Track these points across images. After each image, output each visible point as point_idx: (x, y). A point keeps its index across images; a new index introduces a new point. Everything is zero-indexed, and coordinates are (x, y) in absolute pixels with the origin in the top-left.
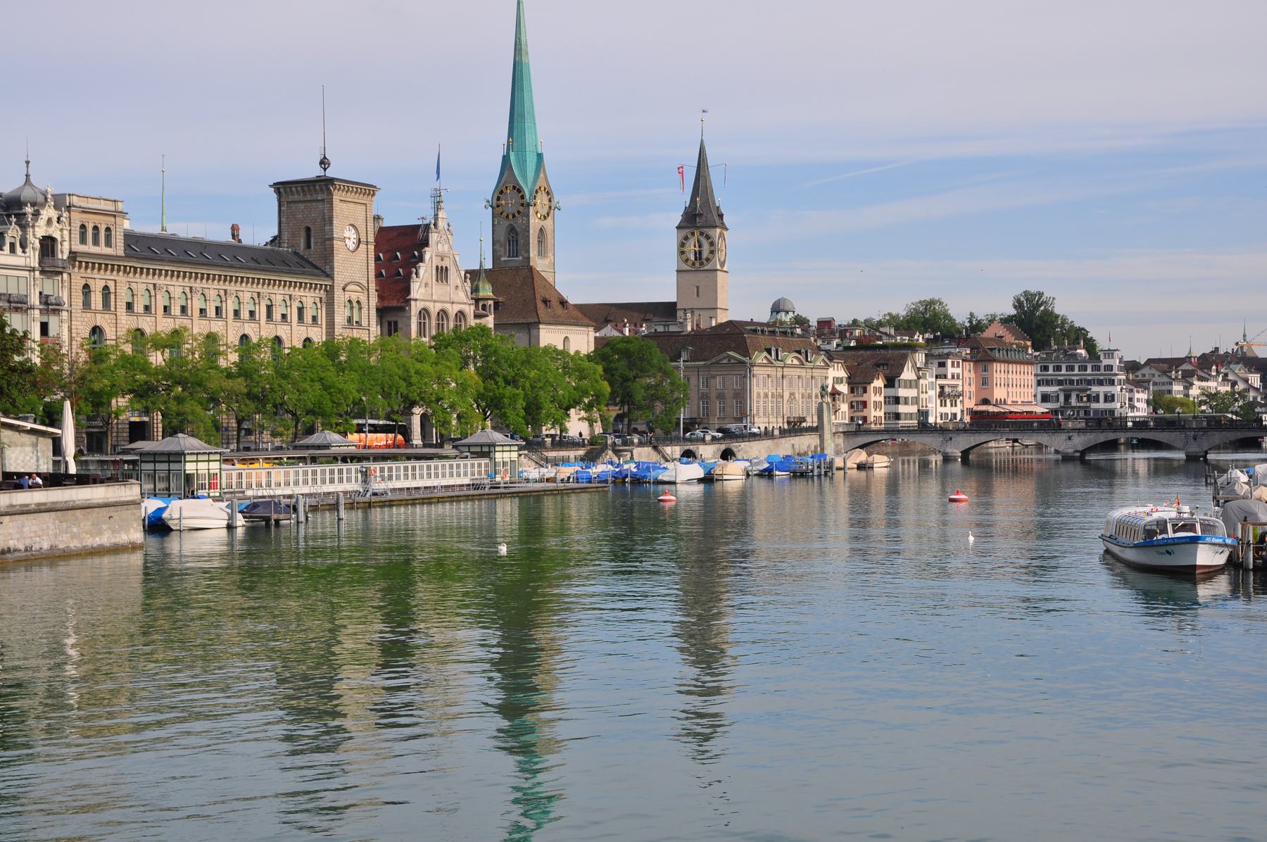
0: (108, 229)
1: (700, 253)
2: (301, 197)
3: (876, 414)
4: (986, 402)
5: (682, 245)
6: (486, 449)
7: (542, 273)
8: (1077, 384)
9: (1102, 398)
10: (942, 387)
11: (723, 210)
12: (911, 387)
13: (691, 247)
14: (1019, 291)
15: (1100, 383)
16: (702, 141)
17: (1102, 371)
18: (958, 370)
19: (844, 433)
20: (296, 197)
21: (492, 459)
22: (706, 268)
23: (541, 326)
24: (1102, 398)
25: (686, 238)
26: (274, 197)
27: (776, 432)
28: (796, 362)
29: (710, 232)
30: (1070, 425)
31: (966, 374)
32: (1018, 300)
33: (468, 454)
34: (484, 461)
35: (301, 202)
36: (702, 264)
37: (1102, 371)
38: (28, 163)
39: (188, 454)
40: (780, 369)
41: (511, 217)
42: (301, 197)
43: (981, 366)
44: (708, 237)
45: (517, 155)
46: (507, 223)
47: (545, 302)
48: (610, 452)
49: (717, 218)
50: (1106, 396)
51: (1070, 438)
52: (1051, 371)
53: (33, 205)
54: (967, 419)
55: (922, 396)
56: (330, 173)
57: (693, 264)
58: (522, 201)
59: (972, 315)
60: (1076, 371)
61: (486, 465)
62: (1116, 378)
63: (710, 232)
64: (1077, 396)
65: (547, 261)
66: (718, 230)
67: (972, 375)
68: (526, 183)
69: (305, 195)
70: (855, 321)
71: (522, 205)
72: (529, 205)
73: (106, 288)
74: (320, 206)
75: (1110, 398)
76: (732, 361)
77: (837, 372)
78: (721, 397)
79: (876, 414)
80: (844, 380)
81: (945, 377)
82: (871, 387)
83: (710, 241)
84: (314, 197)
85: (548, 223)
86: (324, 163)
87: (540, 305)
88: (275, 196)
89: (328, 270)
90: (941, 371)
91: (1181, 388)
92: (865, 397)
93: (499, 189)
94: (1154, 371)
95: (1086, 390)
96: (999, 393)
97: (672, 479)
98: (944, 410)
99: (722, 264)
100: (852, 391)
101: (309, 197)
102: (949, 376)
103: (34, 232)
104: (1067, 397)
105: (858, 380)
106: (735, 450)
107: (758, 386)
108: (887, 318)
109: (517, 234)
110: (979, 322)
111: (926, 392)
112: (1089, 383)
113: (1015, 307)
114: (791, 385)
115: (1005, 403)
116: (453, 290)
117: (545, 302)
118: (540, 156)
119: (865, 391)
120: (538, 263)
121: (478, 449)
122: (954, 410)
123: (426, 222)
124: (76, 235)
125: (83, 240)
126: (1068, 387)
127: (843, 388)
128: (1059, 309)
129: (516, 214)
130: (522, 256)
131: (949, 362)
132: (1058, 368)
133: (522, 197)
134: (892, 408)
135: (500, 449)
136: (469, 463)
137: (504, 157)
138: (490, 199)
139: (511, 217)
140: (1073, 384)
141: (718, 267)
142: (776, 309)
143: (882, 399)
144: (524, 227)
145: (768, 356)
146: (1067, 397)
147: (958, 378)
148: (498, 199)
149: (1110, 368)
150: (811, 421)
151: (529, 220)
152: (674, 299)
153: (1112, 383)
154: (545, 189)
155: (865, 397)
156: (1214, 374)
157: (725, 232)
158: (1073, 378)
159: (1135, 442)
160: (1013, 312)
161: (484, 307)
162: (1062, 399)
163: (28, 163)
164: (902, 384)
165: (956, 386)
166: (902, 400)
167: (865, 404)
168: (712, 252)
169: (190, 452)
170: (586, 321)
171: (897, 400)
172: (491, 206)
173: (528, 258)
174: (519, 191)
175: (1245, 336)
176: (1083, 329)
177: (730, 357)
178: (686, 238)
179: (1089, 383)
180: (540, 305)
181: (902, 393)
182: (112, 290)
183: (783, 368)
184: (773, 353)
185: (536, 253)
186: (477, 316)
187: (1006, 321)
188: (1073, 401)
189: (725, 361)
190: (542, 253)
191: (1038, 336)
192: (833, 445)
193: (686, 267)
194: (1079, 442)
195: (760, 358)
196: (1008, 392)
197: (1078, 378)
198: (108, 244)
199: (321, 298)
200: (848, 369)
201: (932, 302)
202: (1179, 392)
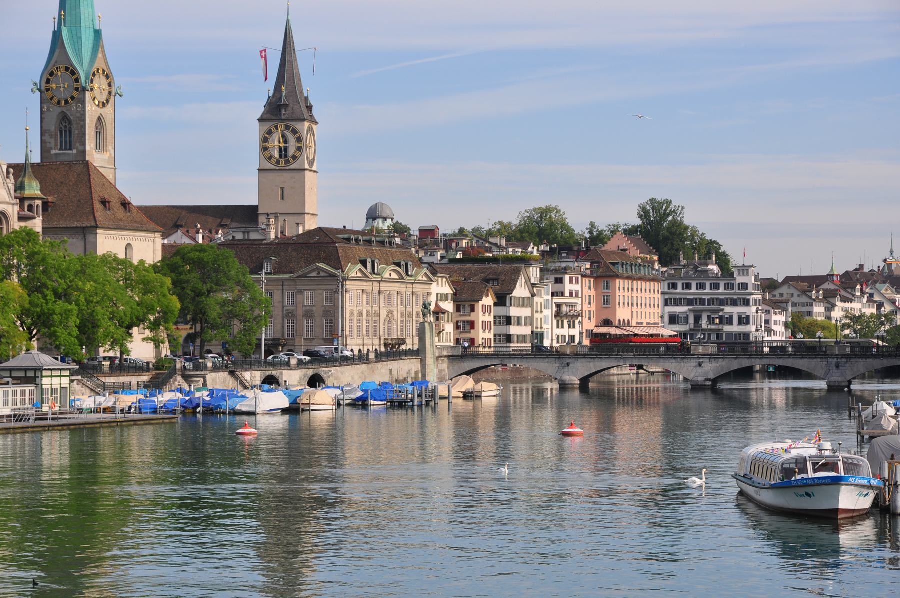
1: (286, 149)
3: (484, 336)
4: (607, 323)
5: (265, 140)
6: (31, 374)
7: (100, 170)
8: (709, 304)
9: (735, 320)
10: (559, 306)
11: (312, 101)
12: (524, 306)
13: (276, 142)
14: (644, 199)
15: (734, 303)
16: (288, 21)
17: (736, 290)
18: (577, 287)
19: (449, 357)
21: (39, 386)
22: (292, 167)
23: (99, 231)
24: (735, 320)
25: (270, 132)
27: (372, 356)
28: (395, 276)
29: (298, 126)
30: (701, 350)
31: (586, 292)
32: (644, 209)
33: (10, 380)
34: (28, 388)
36: (287, 162)
37: (736, 290)
39: (46, 369)
40: (376, 284)
41: (63, 103)
43: (602, 283)
44: (295, 132)
45: (70, 31)
46: (59, 110)
47: (104, 203)
48: (179, 378)
49: (305, 110)
50: (740, 318)
51: (700, 365)
52: (679, 290)
54: (587, 342)
55: (536, 316)
57: (278, 162)
58: (76, 85)
59: (592, 225)
60: (708, 290)
61: (31, 393)
62: (751, 298)
63: (298, 126)
64: (709, 317)
65: (106, 156)
66: (307, 124)
67: (593, 293)
68: (81, 63)
70: (462, 231)
71: (77, 89)
72: (84, 90)
75: (744, 320)
76: (322, 274)
77: (442, 287)
78: (309, 315)
79: (484, 336)
80: (450, 297)
81: (563, 294)
82: (479, 306)
83: (297, 136)
85: (108, 112)
87: (98, 206)
90: (558, 287)
91: (822, 310)
92: (472, 317)
93: (49, 71)
94: (793, 291)
95: (718, 311)
96: (622, 314)
97: (252, 409)
98: (560, 332)
99: (311, 163)
100: (458, 309)
102: (567, 294)
104: (698, 319)
105: (465, 297)
106: (324, 376)
107: (351, 302)
108: (498, 227)
109: (70, 123)
110: (601, 233)
111: (541, 312)
112: (722, 303)
113: (640, 217)
114: (389, 302)
115: (629, 324)
117: (104, 203)
118: (98, 34)
119: (473, 310)
120: (96, 158)
121: (22, 374)
122: (573, 332)
126: (699, 307)
127: (449, 306)
128: (689, 220)
129: (70, 100)
130: (77, 149)
131: (567, 278)
132: (688, 286)
133: (77, 80)
134: (503, 330)
135: (49, 374)
136: (10, 390)
137: (55, 33)
138: (38, 82)
139: (63, 103)
140: (704, 304)
141: (307, 167)
142: (373, 215)
143: (492, 319)
144: (78, 115)
145: (364, 269)
146: (698, 319)
147: (577, 296)
148: (48, 81)
149: (744, 286)
150: (412, 344)
151: (84, 108)
152: (253, 201)
153: (747, 303)
154: (104, 71)
155: (472, 317)
156: (858, 294)
157: (314, 127)
158: (704, 297)
159: (772, 369)
160: (638, 222)
161: (30, 208)
162: (691, 320)
164: (514, 302)
165: (573, 306)
166: (514, 321)
167: (472, 325)
168: (299, 149)
169: (47, 368)
170: (153, 226)
171: (508, 321)
172: (40, 90)
173: (84, 152)
174: (73, 73)
175: (892, 252)
176: (715, 242)
177: (319, 270)
178: (270, 132)
179: (722, 303)
180: (98, 206)
181: (514, 312)
183: (379, 282)
184: (369, 265)
185: (93, 145)
186: (21, 219)
187: (630, 232)
188: (704, 324)
189: (314, 274)
190: (100, 146)
191: (666, 250)
192: (436, 371)
193: (269, 166)
194: (711, 369)
195: (354, 271)
196: (632, 312)
197: (709, 297)
200: (454, 284)
201: (548, 210)
202: (819, 314)
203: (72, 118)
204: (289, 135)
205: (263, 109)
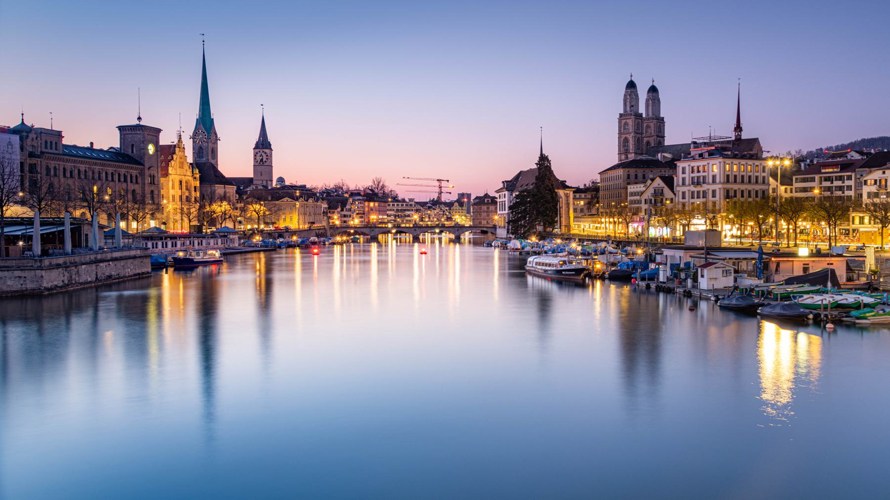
0: (56, 143)
2: (130, 132)
5: (255, 156)
11: (271, 143)
20: (128, 132)
26: (118, 132)
28: (311, 201)
35: (130, 134)
38: (23, 114)
42: (130, 132)
44: (265, 153)
53: (26, 132)
56: (142, 123)
57: (260, 163)
69: (132, 131)
71: (205, 138)
73: (55, 167)
74: (139, 136)
84: (136, 132)
86: (139, 118)
88: (119, 131)
89: (142, 161)
101: (133, 132)
103: (26, 143)
116: (185, 171)
123: (174, 144)
124: (43, 145)
125: (46, 148)
163: (23, 114)
168: (267, 159)
178: (257, 153)
182: (57, 168)
193: (256, 164)
198: (56, 149)
199: (139, 173)
203: (204, 148)
204: (263, 154)
205: (254, 146)
